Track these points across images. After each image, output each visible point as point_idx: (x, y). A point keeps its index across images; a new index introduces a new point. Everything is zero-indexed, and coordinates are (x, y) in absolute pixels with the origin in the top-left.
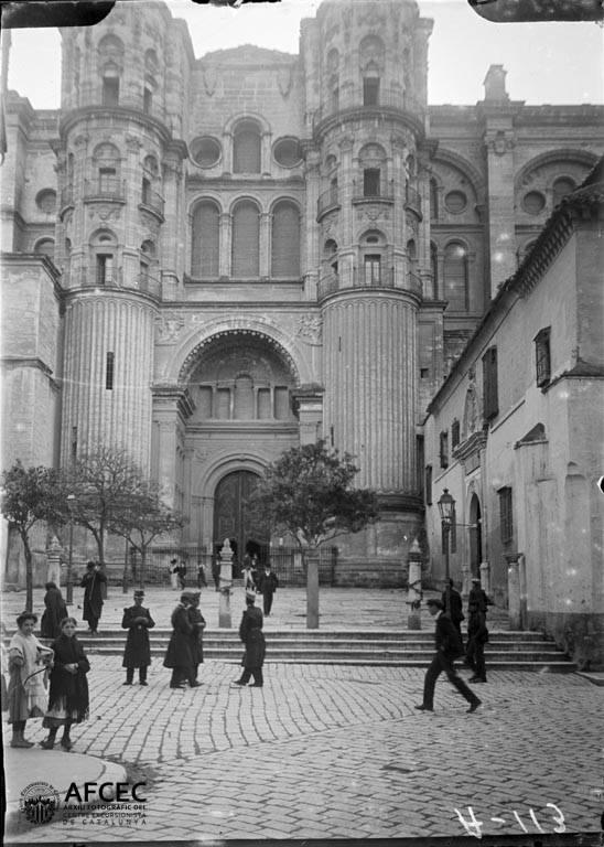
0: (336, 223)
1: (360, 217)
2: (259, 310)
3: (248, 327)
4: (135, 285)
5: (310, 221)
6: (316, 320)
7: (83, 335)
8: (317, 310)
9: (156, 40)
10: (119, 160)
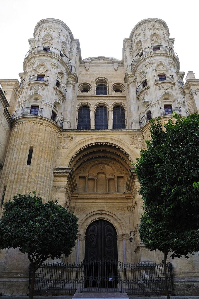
1: (160, 89)
8: (141, 133)
10: (47, 71)
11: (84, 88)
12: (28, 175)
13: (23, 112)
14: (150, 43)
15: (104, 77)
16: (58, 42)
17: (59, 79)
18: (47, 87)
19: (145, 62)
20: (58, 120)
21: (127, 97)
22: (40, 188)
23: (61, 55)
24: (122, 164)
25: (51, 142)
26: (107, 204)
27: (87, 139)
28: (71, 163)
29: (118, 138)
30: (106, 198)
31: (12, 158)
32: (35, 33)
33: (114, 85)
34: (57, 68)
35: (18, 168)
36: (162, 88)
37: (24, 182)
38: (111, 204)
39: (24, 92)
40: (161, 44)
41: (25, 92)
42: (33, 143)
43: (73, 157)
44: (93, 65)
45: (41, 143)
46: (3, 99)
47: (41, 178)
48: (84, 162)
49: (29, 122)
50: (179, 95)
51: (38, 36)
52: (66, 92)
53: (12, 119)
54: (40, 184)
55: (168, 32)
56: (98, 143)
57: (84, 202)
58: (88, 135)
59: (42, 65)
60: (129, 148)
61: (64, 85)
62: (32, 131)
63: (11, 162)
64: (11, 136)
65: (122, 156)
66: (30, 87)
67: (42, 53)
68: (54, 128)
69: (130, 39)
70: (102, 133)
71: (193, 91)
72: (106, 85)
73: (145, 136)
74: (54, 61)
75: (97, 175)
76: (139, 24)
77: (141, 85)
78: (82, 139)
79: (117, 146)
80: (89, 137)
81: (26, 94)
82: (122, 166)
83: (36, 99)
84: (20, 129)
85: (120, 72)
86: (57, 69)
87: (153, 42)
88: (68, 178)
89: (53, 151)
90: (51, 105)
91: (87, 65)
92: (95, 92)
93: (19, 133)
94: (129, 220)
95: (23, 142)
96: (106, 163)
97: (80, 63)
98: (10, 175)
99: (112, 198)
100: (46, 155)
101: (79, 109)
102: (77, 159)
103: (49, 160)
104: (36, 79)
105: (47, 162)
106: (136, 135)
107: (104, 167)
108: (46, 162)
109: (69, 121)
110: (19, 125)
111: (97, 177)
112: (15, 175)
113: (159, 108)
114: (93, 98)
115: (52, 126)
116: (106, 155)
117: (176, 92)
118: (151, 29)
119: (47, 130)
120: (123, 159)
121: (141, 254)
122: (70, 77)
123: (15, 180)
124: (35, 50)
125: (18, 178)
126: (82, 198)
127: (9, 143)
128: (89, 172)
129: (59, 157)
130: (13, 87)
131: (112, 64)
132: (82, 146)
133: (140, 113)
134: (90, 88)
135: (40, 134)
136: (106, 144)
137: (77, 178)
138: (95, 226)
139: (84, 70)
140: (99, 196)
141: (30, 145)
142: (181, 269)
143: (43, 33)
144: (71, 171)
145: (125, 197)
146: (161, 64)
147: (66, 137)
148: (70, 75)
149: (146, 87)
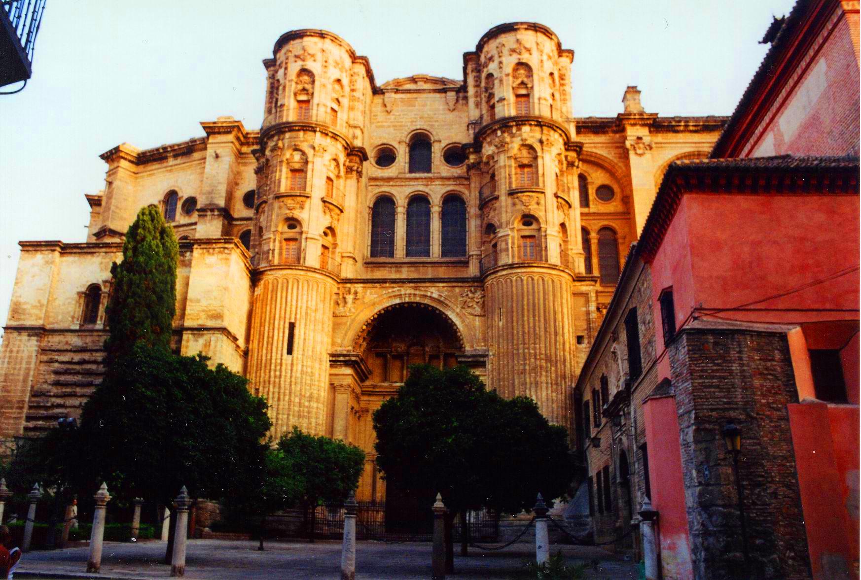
0: (495, 210)
2: (427, 285)
3: (418, 299)
4: (317, 266)
5: (472, 210)
6: (478, 294)
7: (268, 308)
8: (482, 285)
9: (341, 71)
15: (425, 127)
18: (309, 199)
83: (291, 227)
106: (473, 289)
109: (351, 255)
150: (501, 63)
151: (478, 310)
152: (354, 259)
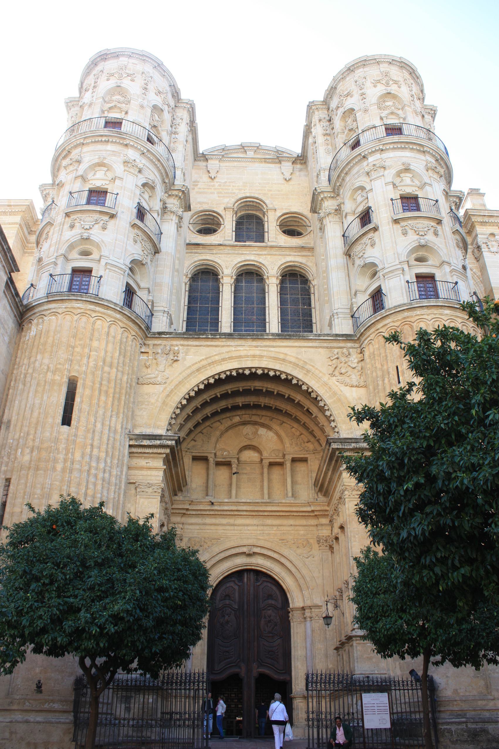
1: (405, 234)
6: (354, 358)
8: (357, 345)
10: (113, 180)
11: (202, 224)
12: (64, 452)
13: (50, 285)
14: (379, 118)
15: (256, 196)
16: (142, 107)
17: (142, 200)
18: (112, 222)
19: (365, 163)
20: (139, 307)
21: (320, 250)
22: (95, 484)
23: (149, 140)
24: (304, 426)
25: (121, 365)
26: (265, 528)
27: (217, 358)
28: (173, 422)
29: (297, 358)
30: (261, 514)
31: (23, 407)
32: (82, 83)
33: (283, 218)
34: (140, 171)
35: (39, 432)
36: (410, 232)
37: (54, 469)
38: (275, 528)
39: (54, 234)
40: (404, 119)
41: (56, 235)
42: (76, 367)
43: (180, 406)
44: (227, 164)
45: (96, 367)
46: (5, 253)
47: (98, 459)
48: (206, 419)
49: (68, 312)
50: (452, 249)
51: (91, 91)
52: (162, 233)
53: (22, 305)
54: (96, 476)
55: (422, 91)
56: (244, 369)
57: (204, 524)
58: (217, 349)
59: (101, 164)
60: (325, 384)
61: (155, 215)
62: (75, 336)
63: (21, 417)
64: (20, 348)
65: (307, 404)
66: (69, 221)
67: (102, 136)
68: (130, 327)
69: (326, 103)
70: (255, 343)
71: (481, 239)
72: (261, 216)
73: (367, 354)
74: (132, 154)
75: (238, 454)
76: (349, 69)
77: (357, 222)
78: (203, 358)
79: (293, 377)
80: (220, 354)
81: (60, 239)
82: (304, 432)
83: (86, 253)
84: (44, 331)
85: (299, 184)
86: (139, 175)
87: (384, 114)
88: (166, 461)
89: (128, 389)
90: (123, 267)
91: (213, 164)
92: (234, 233)
93: (42, 341)
94: (321, 571)
95: (51, 365)
96: (262, 421)
97: (195, 160)
98: (20, 450)
99: (278, 514)
100: (111, 399)
101: (192, 277)
102: (189, 410)
103: (118, 414)
104: (84, 201)
105: (114, 419)
106: (345, 350)
107: (256, 433)
108: (111, 417)
109: (166, 310)
110: (41, 320)
111: (238, 459)
112: (32, 451)
113: (403, 283)
114: (227, 250)
115: (126, 324)
116: (263, 401)
117: (445, 242)
118: (379, 81)
119: (113, 334)
120: (308, 412)
121: (355, 655)
122: (170, 195)
123: (32, 463)
124: (84, 128)
125: (39, 459)
126: (199, 513)
127: (16, 367)
128: (218, 446)
129: (144, 406)
130: (17, 219)
131: (276, 163)
132: (202, 377)
133: (353, 292)
134: (219, 225)
135: (95, 344)
136: (266, 371)
137: (187, 460)
138: (232, 584)
139: (205, 178)
140: (244, 508)
141: (69, 371)
142: (457, 690)
143: (105, 85)
144: (174, 442)
145: (313, 511)
146: (407, 170)
147: (160, 351)
148: (170, 189)
149: (370, 226)
150: (363, 94)
151: (354, 378)
152: (171, 316)
